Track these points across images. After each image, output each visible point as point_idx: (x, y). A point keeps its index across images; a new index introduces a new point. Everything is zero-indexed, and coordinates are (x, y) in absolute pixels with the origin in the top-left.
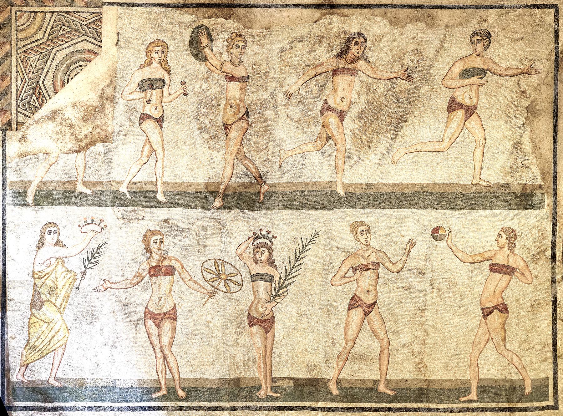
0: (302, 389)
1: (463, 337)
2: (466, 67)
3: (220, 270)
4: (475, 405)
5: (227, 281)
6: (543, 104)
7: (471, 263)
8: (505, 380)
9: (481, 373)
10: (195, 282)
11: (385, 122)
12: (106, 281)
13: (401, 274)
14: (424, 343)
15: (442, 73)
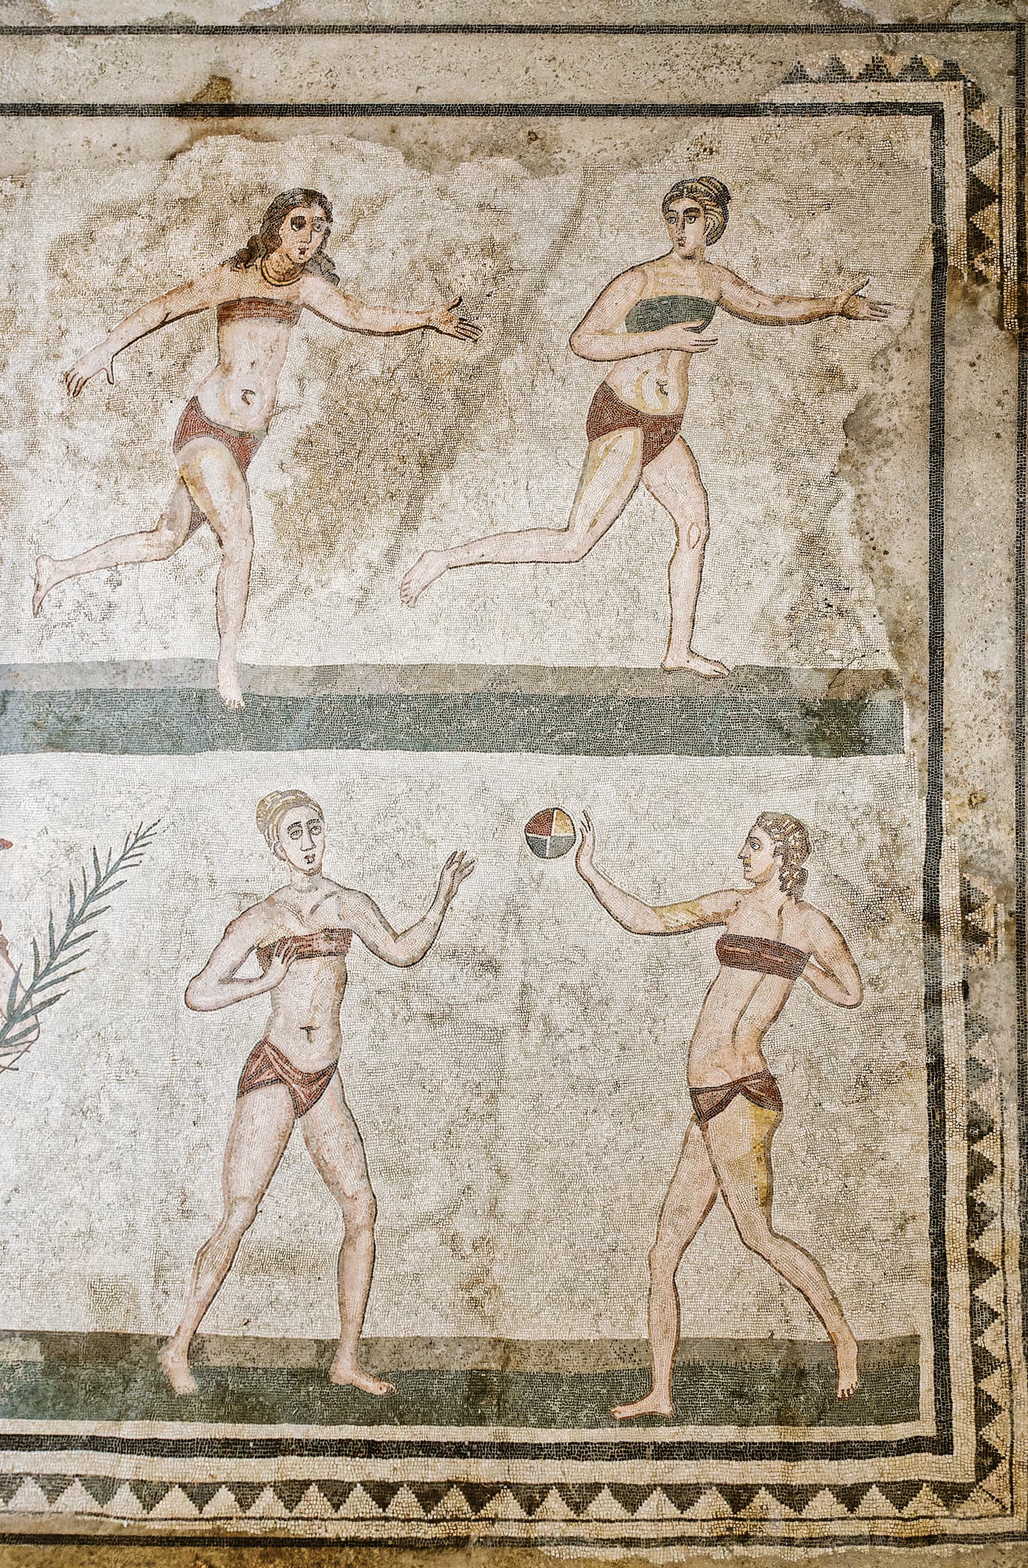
0: (72, 1371)
1: (624, 1190)
2: (651, 293)
4: (664, 1434)
6: (895, 414)
7: (657, 934)
8: (769, 1343)
9: (687, 1317)
11: (382, 466)
13: (422, 971)
14: (493, 1211)
15: (571, 313)
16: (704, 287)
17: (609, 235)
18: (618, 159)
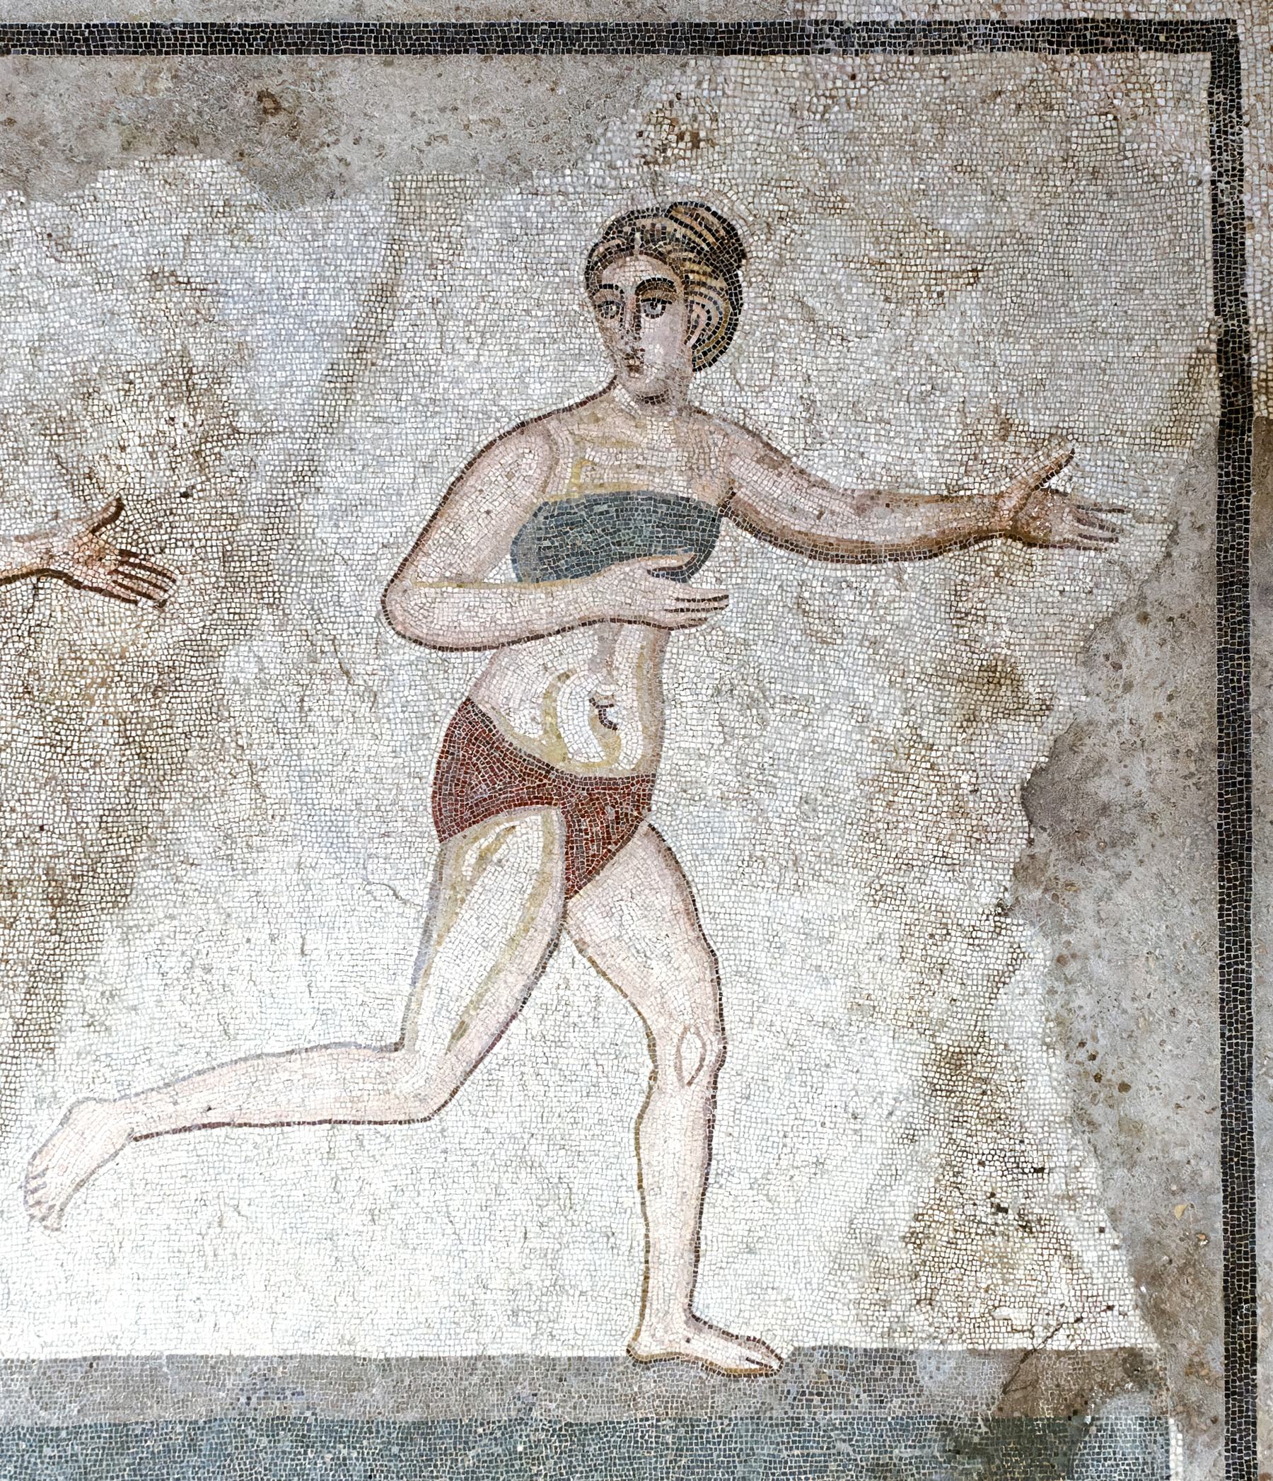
6: (1138, 768)
15: (383, 534)
16: (691, 471)
17: (462, 347)
18: (475, 160)
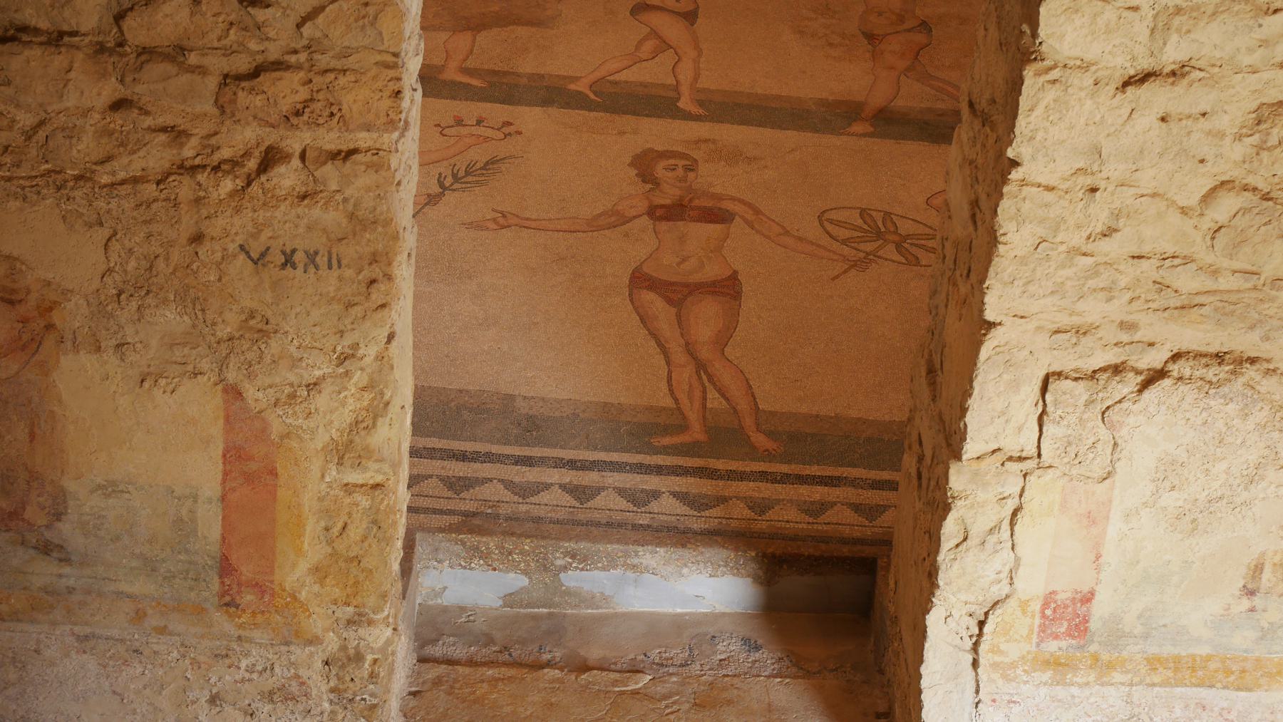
3: (881, 225)
5: (906, 245)
10: (800, 239)
12: (508, 215)
